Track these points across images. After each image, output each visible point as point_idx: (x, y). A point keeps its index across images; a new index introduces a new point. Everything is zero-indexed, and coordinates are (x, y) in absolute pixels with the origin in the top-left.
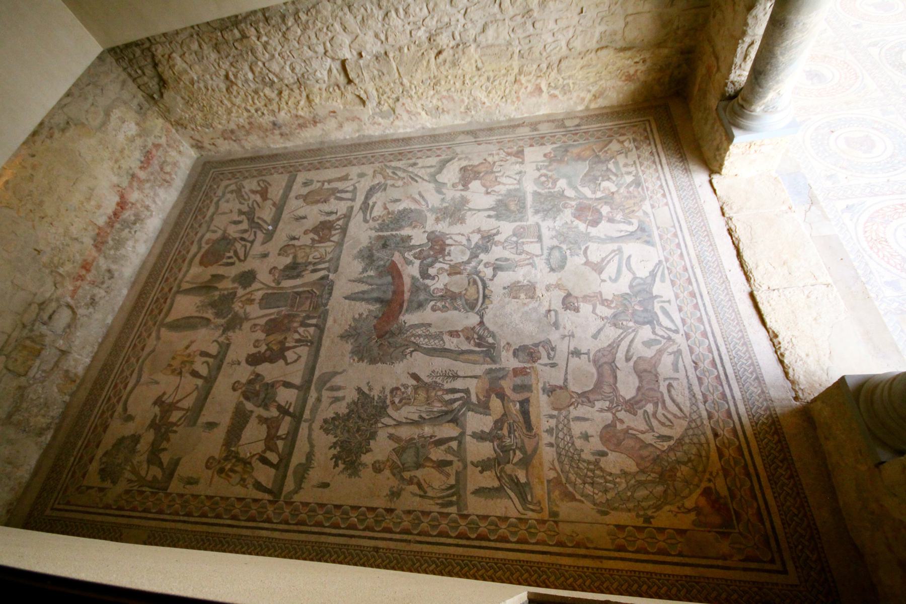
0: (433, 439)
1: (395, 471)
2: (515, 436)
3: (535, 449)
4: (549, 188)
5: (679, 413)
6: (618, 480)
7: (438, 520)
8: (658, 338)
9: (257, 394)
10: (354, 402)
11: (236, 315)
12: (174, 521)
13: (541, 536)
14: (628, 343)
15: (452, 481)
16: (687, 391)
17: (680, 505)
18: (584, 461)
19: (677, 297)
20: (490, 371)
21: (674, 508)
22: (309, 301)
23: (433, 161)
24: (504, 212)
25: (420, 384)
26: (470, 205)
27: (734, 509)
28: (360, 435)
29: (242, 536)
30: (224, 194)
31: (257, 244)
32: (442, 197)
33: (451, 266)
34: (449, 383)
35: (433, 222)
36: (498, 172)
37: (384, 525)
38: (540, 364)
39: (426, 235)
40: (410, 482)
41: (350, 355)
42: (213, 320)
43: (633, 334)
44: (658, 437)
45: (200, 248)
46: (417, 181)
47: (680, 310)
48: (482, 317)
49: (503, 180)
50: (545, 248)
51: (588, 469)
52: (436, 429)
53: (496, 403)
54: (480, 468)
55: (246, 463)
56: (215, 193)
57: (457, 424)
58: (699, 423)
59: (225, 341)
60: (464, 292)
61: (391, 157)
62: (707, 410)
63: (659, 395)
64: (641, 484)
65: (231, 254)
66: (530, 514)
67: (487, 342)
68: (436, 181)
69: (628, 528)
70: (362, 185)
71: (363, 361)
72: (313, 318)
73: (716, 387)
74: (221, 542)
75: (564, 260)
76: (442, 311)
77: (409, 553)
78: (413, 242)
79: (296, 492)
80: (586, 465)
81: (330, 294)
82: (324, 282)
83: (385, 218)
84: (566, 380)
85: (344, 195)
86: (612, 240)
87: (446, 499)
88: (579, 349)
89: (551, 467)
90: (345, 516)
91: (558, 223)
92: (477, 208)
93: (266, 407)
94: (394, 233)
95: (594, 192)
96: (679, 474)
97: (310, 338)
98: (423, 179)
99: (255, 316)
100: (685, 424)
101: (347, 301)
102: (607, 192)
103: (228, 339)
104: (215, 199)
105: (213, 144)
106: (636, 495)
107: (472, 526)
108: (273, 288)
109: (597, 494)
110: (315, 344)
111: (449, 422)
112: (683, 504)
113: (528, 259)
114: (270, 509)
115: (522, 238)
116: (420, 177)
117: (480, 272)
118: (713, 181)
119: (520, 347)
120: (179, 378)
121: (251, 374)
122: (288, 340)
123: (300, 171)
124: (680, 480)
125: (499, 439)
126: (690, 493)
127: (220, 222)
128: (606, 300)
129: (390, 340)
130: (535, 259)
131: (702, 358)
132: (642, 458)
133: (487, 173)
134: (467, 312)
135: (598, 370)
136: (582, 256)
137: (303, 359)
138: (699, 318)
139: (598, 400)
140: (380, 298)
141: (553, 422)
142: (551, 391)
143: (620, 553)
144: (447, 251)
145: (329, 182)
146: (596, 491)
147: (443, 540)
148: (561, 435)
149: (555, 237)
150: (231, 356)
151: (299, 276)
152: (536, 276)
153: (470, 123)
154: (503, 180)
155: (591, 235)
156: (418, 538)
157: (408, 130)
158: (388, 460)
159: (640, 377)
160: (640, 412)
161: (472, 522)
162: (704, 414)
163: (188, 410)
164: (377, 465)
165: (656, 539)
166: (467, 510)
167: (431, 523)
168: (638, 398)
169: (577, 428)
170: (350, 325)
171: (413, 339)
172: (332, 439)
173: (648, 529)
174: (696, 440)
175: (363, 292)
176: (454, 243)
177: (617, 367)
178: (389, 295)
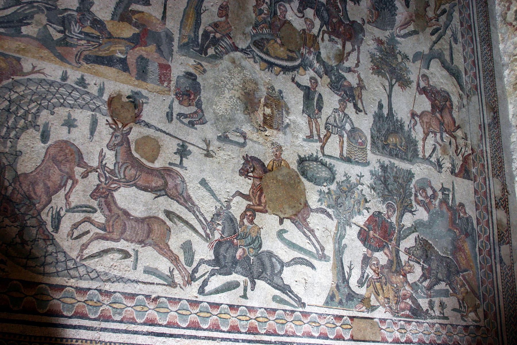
2: (81, 39)
3: (62, 58)
4: (416, 196)
5: (87, 252)
6: (9, 144)
8: (195, 265)
14: (191, 222)
16: (116, 273)
19: (251, 309)
20: (170, 37)
23: (459, 62)
24: (386, 126)
32: (411, 57)
33: (315, 37)
36: (441, 137)
38: (173, 102)
43: (203, 233)
44: (58, 213)
46: (432, 34)
47: (232, 307)
48: (242, 51)
49: (431, 141)
51: (27, 112)
58: (72, 272)
61: (465, 15)
62: (89, 289)
63: (115, 236)
67: (208, 47)
73: (120, 314)
80: (33, 111)
84: (148, 125)
86: (339, 252)
88: (188, 157)
89: (36, 69)
92: (393, 94)
95: (408, 251)
96: (7, 221)
98: (435, 43)
100: (74, 254)
102: (407, 268)
113: (319, 136)
115: (348, 137)
117: (305, 70)
119: (199, 84)
125: (80, 19)
128: (254, 216)
130: (319, 144)
131: (162, 310)
132: (34, 183)
134: (252, 37)
135: (157, 170)
138: (219, 327)
139: (116, 155)
141: (94, 90)
144: (336, 39)
148: (75, 94)
153: (509, 125)
154: (431, 141)
155: (348, 228)
157: (501, 46)
159: (143, 220)
160: (94, 204)
162: (84, 284)
168: (113, 207)
176: (346, 51)
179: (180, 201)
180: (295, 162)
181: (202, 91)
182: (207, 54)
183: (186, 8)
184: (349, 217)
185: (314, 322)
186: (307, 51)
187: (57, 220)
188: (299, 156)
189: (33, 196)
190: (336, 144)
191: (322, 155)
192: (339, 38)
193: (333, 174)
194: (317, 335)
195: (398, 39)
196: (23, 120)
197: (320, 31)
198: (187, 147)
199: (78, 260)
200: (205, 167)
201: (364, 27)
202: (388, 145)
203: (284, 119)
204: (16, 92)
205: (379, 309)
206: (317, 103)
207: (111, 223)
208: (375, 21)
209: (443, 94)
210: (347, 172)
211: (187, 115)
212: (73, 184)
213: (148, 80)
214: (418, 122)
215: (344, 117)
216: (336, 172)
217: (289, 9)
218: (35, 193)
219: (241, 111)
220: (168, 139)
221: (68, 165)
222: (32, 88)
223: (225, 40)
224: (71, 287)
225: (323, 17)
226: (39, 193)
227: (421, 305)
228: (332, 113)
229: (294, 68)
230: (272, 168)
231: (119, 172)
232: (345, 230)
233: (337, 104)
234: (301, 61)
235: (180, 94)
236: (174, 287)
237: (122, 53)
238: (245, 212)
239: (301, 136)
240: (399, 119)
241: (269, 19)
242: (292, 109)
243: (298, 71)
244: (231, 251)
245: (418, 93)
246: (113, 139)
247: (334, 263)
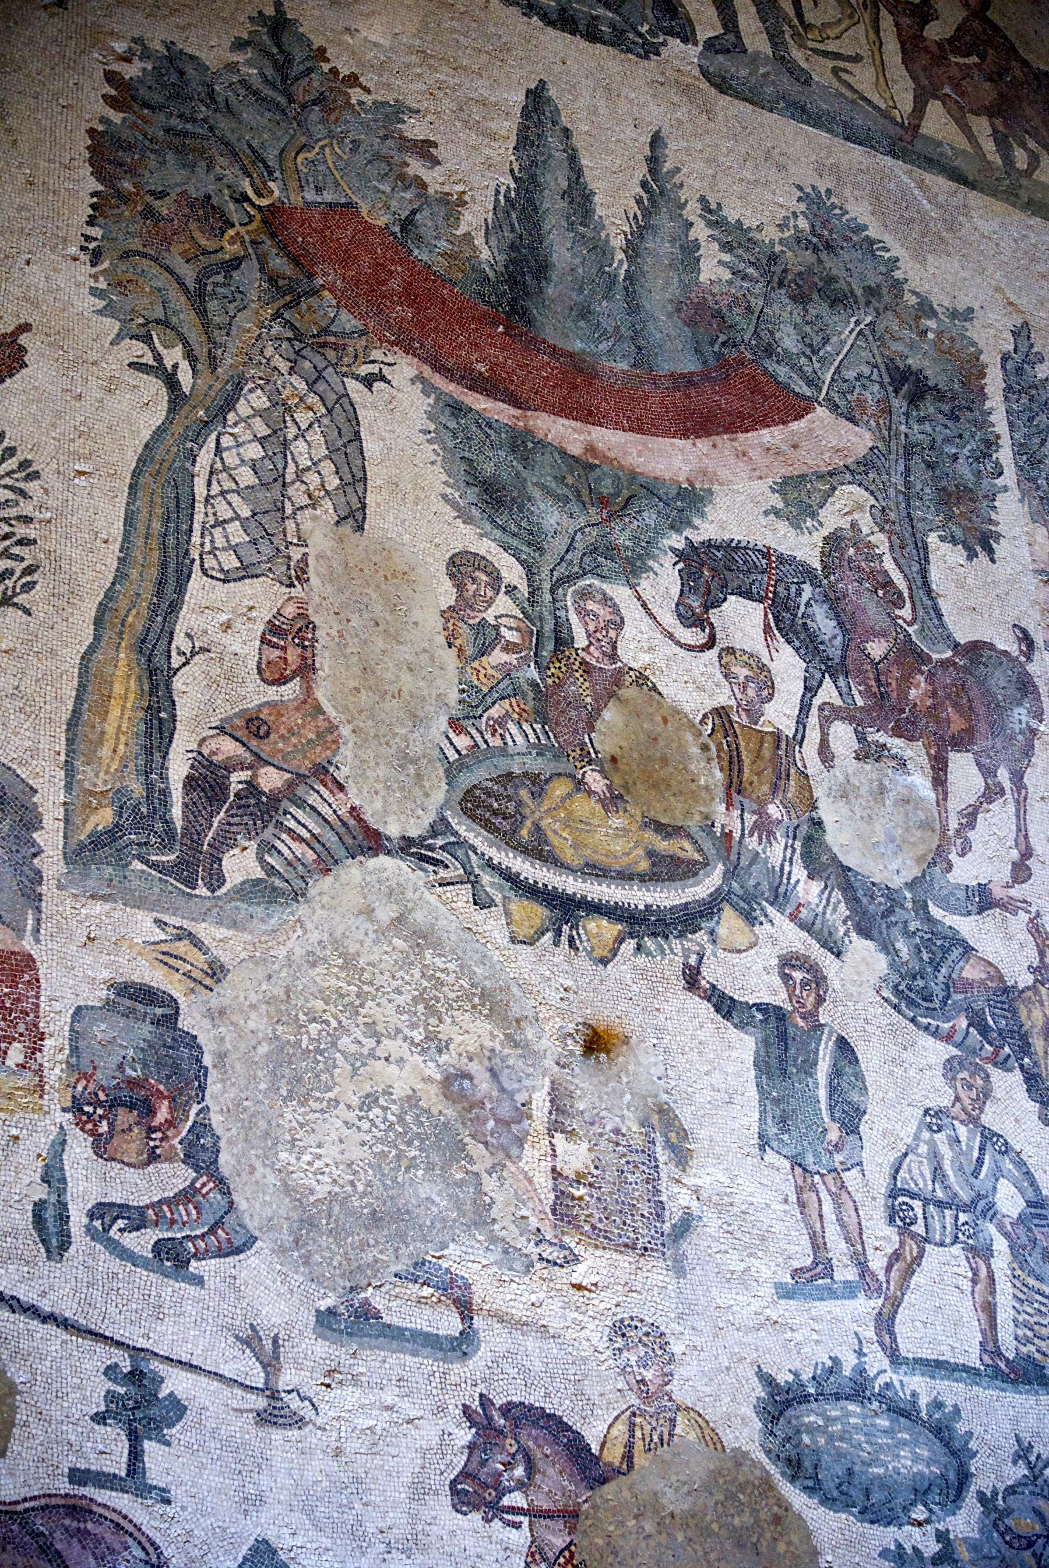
39: (1006, 643)
41: (157, 46)
48: (407, 847)
60: (595, 780)
67: (225, 841)
76: (449, 613)
94: (1005, 455)
101: (518, 98)
115: (1015, 1249)
130: (866, 1306)
134: (452, 771)
144: (896, 744)
152: (728, 1278)
170: (353, 80)
171: (259, 400)
180: (748, 1411)
181: (213, 1075)
182: (222, 881)
183: (91, 650)
186: (750, 819)
188: (768, 1381)
190: (955, 1297)
191: (886, 1363)
192: (911, 739)
193: (954, 1453)
197: (805, 708)
201: (1031, 668)
206: (833, 1090)
210: (1027, 1438)
211: (141, 1210)
215: (982, 1149)
216: (973, 1445)
217: (631, 610)
219: (430, 1167)
220: (55, 1346)
223: (313, 799)
228: (917, 1137)
230: (628, 1456)
233: (940, 1081)
235: (98, 1104)
239: (766, 1273)
241: (533, 673)
242: (703, 1134)
243: (712, 932)
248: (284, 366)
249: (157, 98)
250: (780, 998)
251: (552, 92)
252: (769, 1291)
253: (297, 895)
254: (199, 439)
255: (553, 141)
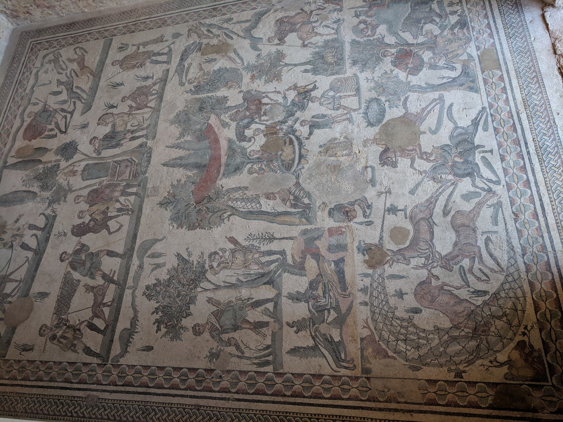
0: (251, 301)
1: (214, 333)
4: (369, 36)
5: (496, 267)
6: (431, 336)
7: (255, 378)
8: (478, 190)
9: (83, 264)
10: (174, 268)
11: (60, 187)
12: (12, 385)
13: (354, 392)
14: (447, 197)
15: (268, 342)
17: (492, 358)
18: (398, 319)
19: (500, 146)
20: (305, 232)
21: (486, 362)
22: (129, 169)
23: (248, 14)
24: (320, 65)
25: (238, 247)
26: (287, 61)
27: (548, 362)
28: (180, 300)
29: (74, 397)
30: (42, 65)
31: (76, 115)
34: (265, 246)
35: (249, 80)
36: (315, 22)
37: (204, 384)
39: (242, 95)
40: (229, 343)
42: (39, 194)
43: (452, 187)
44: (473, 292)
45: (23, 121)
46: (232, 38)
47: (503, 159)
48: (298, 177)
49: (320, 30)
50: (363, 101)
51: (401, 326)
52: (253, 291)
53: (311, 263)
54: (295, 328)
55: (76, 330)
56: (34, 65)
57: (273, 286)
58: (516, 277)
59: (51, 213)
62: (525, 263)
63: (476, 250)
64: (454, 339)
65: (53, 126)
66: (343, 372)
68: (252, 38)
69: (439, 383)
70: (177, 46)
71: (182, 227)
72: (132, 186)
73: (537, 239)
74: (56, 403)
75: (382, 113)
77: (228, 410)
78: (229, 104)
79: (122, 355)
80: (399, 323)
81: (149, 161)
82: (143, 150)
83: (200, 80)
84: (381, 238)
85: (159, 58)
86: (434, 88)
87: (264, 359)
89: (365, 325)
90: (168, 377)
91: (378, 73)
93: (92, 277)
94: (210, 95)
96: (493, 329)
97: (130, 207)
98: (238, 36)
99: (78, 187)
100: (502, 278)
101: (165, 168)
102: (429, 36)
103: (54, 212)
104: (34, 71)
105: (28, 12)
106: (448, 350)
107: (288, 384)
108: (94, 158)
109: (409, 350)
110: (136, 212)
111: (265, 284)
112: (496, 358)
113: (346, 114)
114: (100, 371)
116: (236, 34)
117: (296, 131)
118: (546, 14)
119: (335, 206)
120: (11, 251)
121: (77, 245)
122: (110, 210)
123: (115, 35)
124: (493, 334)
125: (314, 299)
126: (504, 347)
127: (41, 94)
129: (207, 205)
130: (353, 113)
132: (456, 314)
133: (303, 24)
136: (401, 107)
137: (125, 229)
138: (522, 167)
139: (413, 258)
140: (197, 163)
141: (367, 281)
142: (366, 249)
143: (431, 407)
144: (263, 110)
145: (145, 44)
146: (409, 348)
147: (259, 397)
148: (375, 293)
149: (374, 88)
150: (58, 227)
151: (118, 145)
152: (352, 132)
154: (320, 30)
155: (412, 84)
156: (236, 396)
158: (207, 323)
159: (456, 231)
160: (456, 268)
161: (287, 380)
162: (522, 267)
163: (20, 281)
164: (197, 328)
165: (467, 392)
166: (282, 368)
167: (249, 382)
168: (455, 253)
169: (392, 286)
170: (169, 192)
172: (154, 304)
173: (460, 383)
174: (512, 294)
175: (181, 158)
176: (270, 102)
177: (434, 222)
178: (206, 160)
179: (433, 207)
184: (403, 84)
185: (495, 98)
187: (478, 293)
188: (367, 126)
189: (466, 313)
194: (505, 96)
195: (245, 64)
196: (409, 328)
198: (388, 208)
199: (505, 274)
200: (400, 193)
201: (245, 91)
202: (335, 62)
203: (341, 141)
204: (389, 337)
205: (469, 52)
207: (468, 254)
208: (237, 83)
209: (278, 25)
212: (446, 285)
213: (345, 242)
214: (308, 41)
218: (463, 311)
221: (433, 291)
222: (381, 326)
223: (293, 191)
224: (527, 276)
225: (248, 123)
226: (462, 309)
227: (456, 21)
229: (298, 138)
231: (425, 253)
232: (414, 85)
233: (315, 104)
234: (290, 134)
236: (501, 202)
237: (330, 265)
238: (425, 160)
240: (311, 56)
241: (265, 162)
244: (459, 166)
245: (285, 44)
246: (400, 261)
247: (444, 90)
248: (223, 200)
249: (180, 221)
250: (308, 126)
251: (163, 163)
252: (353, 127)
253: (309, 193)
254: (239, 211)
255: (172, 162)
